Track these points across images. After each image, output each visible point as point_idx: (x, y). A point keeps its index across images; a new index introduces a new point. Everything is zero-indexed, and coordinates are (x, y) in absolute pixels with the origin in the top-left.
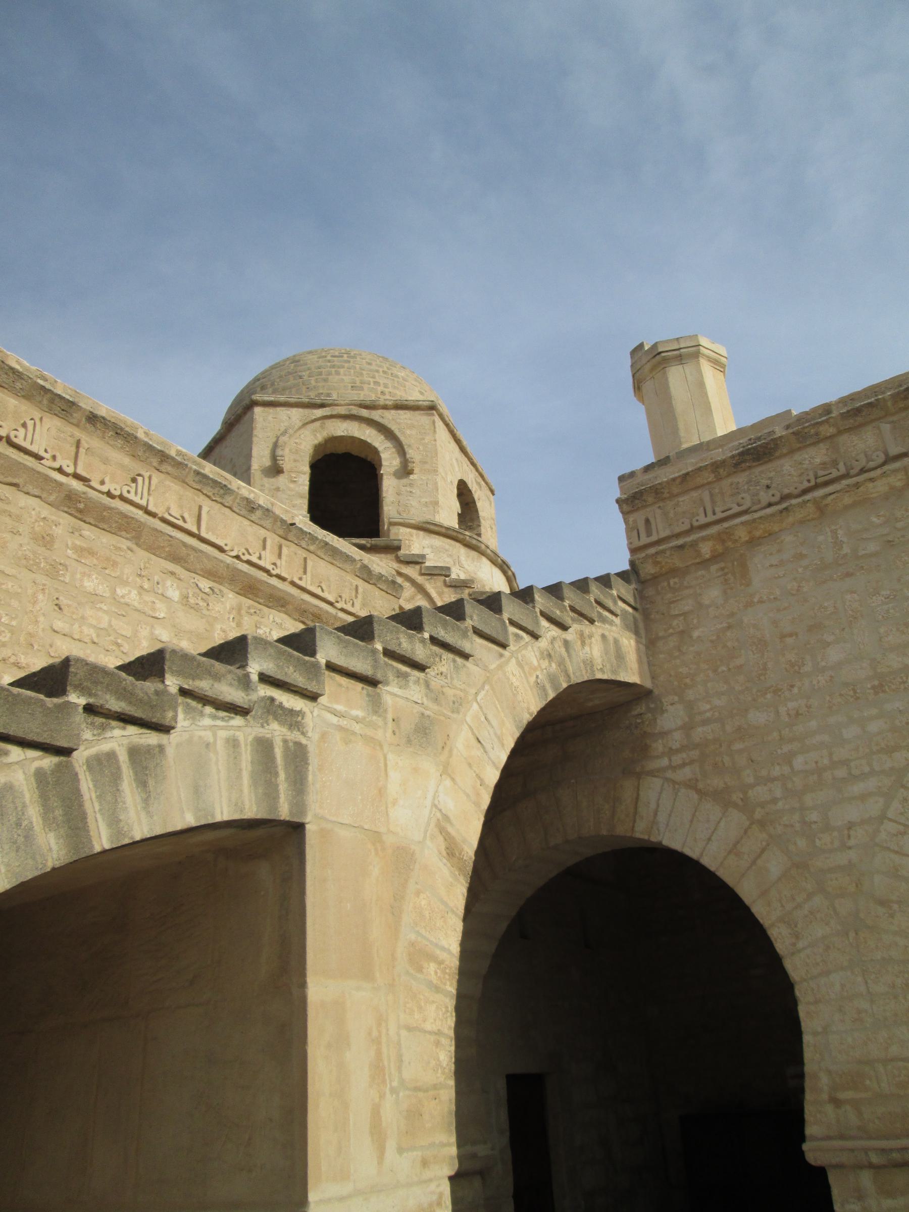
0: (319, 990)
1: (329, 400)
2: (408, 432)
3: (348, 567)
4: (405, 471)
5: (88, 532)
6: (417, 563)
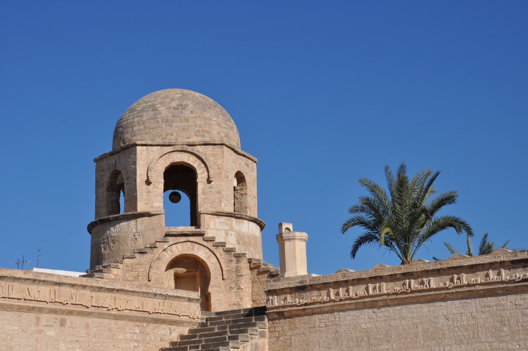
1: (173, 142)
2: (210, 158)
3: (184, 300)
5: (119, 322)
6: (211, 241)
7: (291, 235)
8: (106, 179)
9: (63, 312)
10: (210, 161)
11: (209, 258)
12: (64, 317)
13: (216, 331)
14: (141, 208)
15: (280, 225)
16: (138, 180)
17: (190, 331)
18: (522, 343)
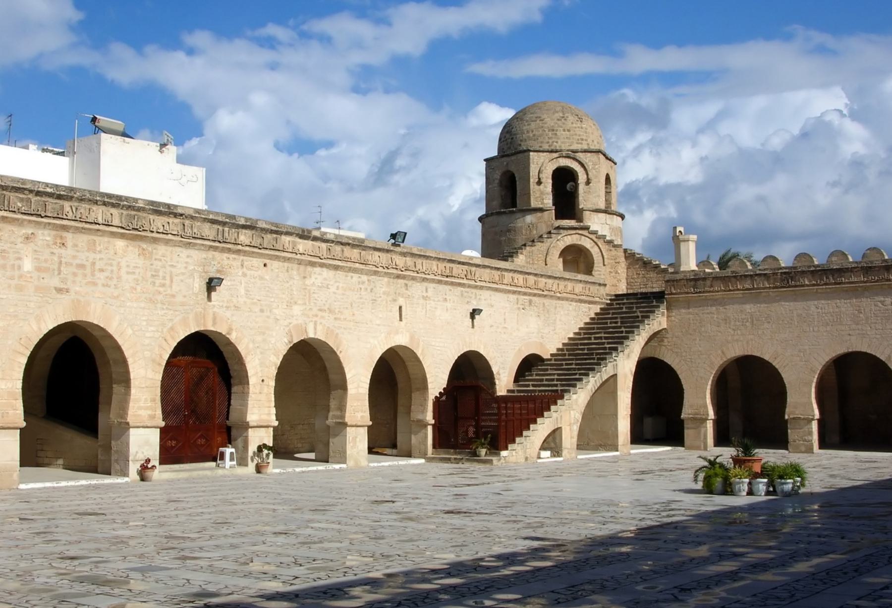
0: (619, 393)
4: (588, 182)
7: (686, 237)
8: (497, 175)
9: (530, 294)
10: (590, 166)
11: (592, 247)
12: (531, 298)
13: (624, 310)
14: (534, 204)
15: (675, 228)
16: (532, 180)
17: (601, 309)
18: (872, 326)
